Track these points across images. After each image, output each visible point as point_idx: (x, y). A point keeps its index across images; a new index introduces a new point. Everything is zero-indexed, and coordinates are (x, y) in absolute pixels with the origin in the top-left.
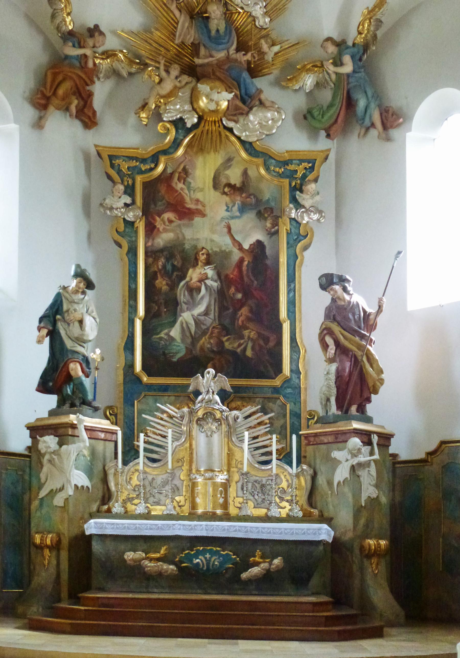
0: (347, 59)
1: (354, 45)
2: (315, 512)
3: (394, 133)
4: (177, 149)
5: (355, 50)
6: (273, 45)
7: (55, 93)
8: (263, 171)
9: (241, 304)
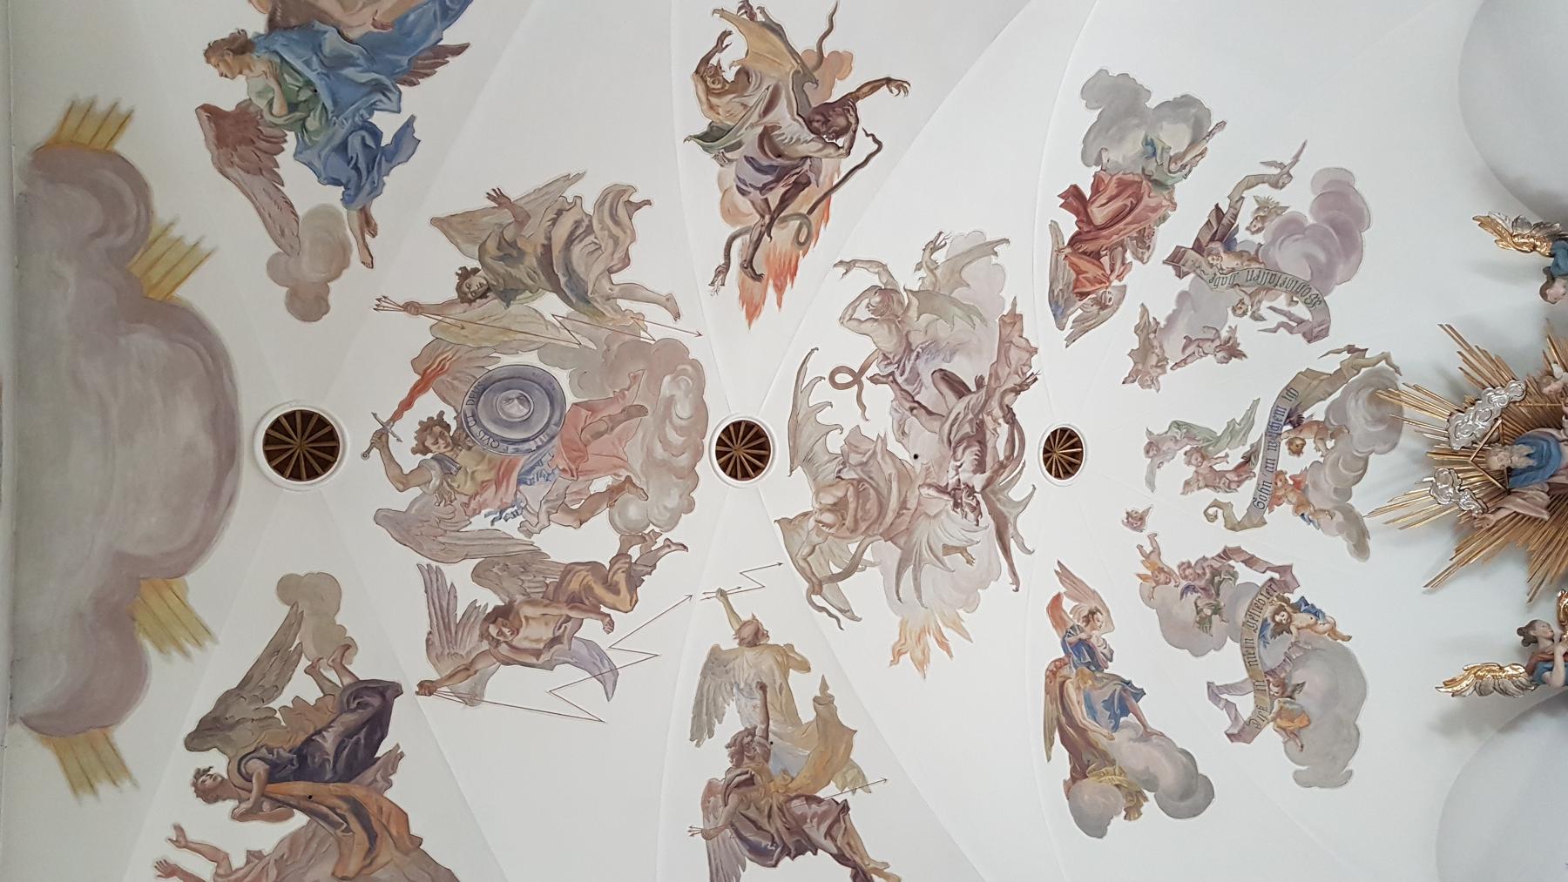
1: (1551, 255)
5: (1560, 253)
6: (1551, 374)
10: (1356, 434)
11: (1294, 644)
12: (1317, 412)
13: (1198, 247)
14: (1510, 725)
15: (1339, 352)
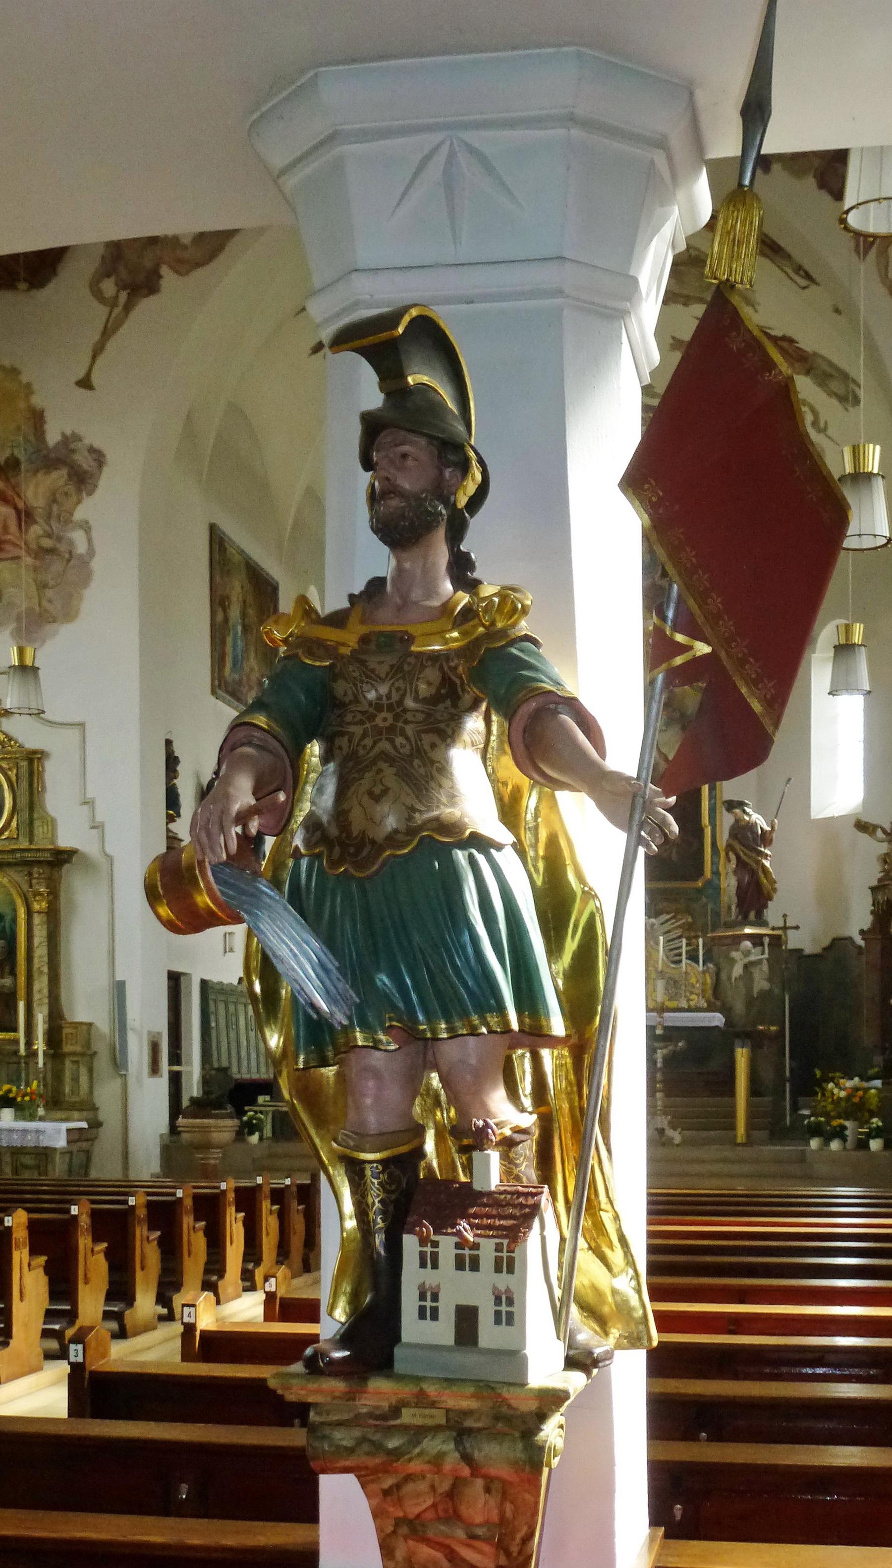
2: (718, 1003)
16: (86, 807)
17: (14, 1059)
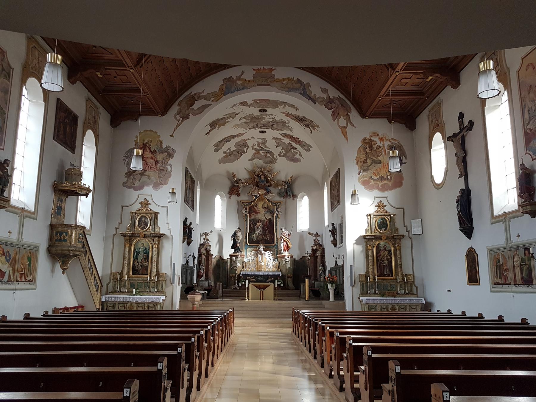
0: (286, 185)
3: (295, 199)
4: (255, 201)
6: (273, 182)
7: (233, 192)
8: (271, 204)
9: (267, 230)
10: (266, 159)
11: (236, 155)
12: (268, 155)
13: (291, 145)
14: (229, 178)
15: (277, 158)
16: (167, 225)
17: (146, 281)
